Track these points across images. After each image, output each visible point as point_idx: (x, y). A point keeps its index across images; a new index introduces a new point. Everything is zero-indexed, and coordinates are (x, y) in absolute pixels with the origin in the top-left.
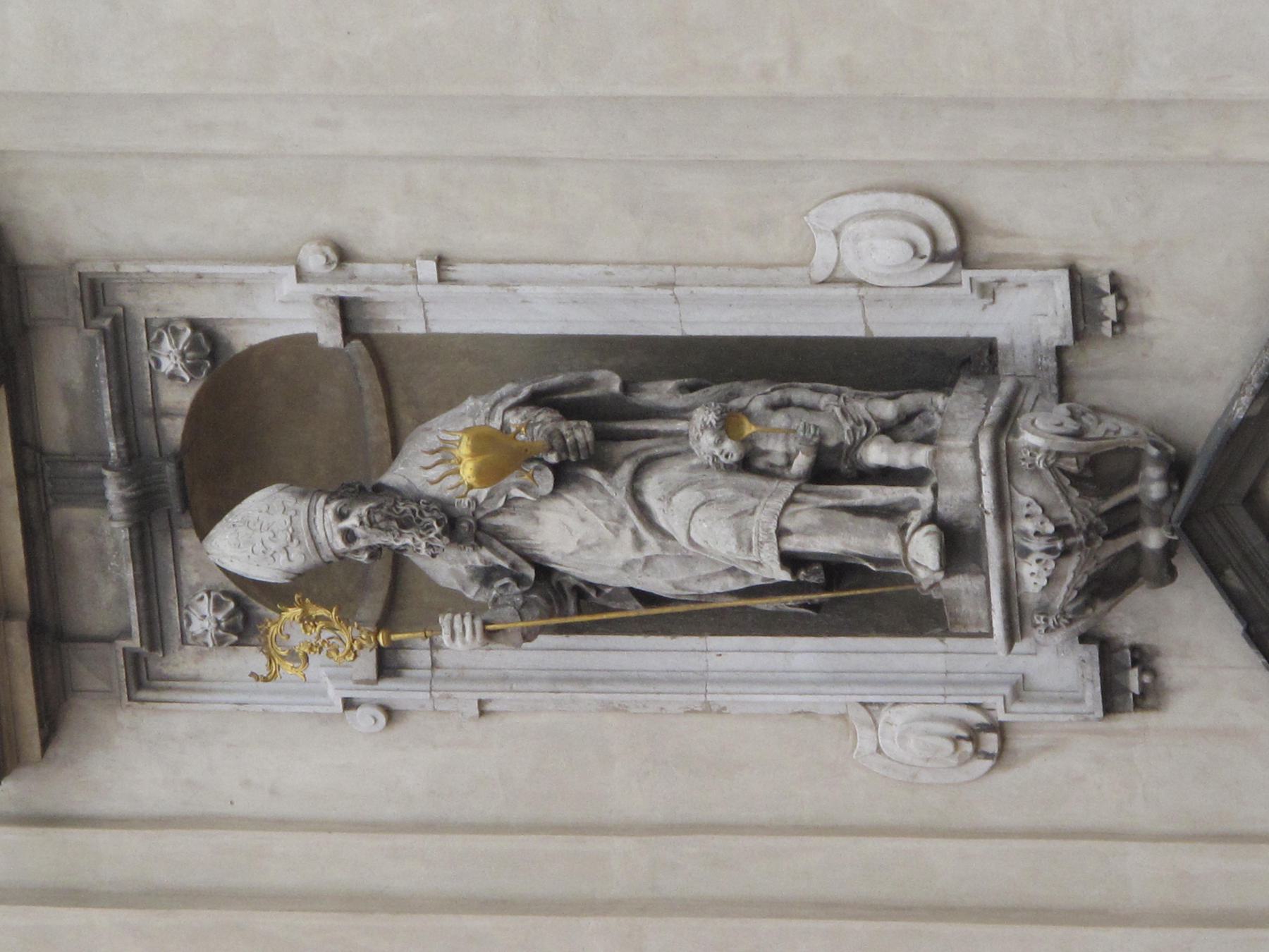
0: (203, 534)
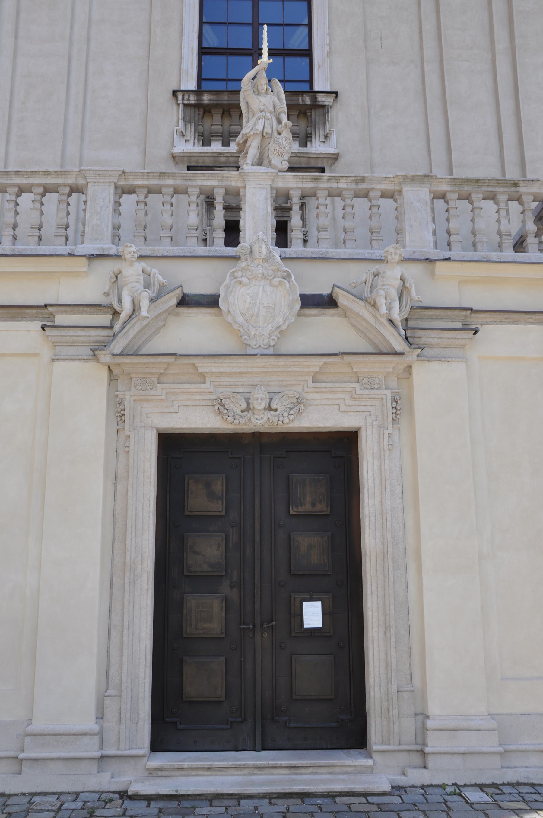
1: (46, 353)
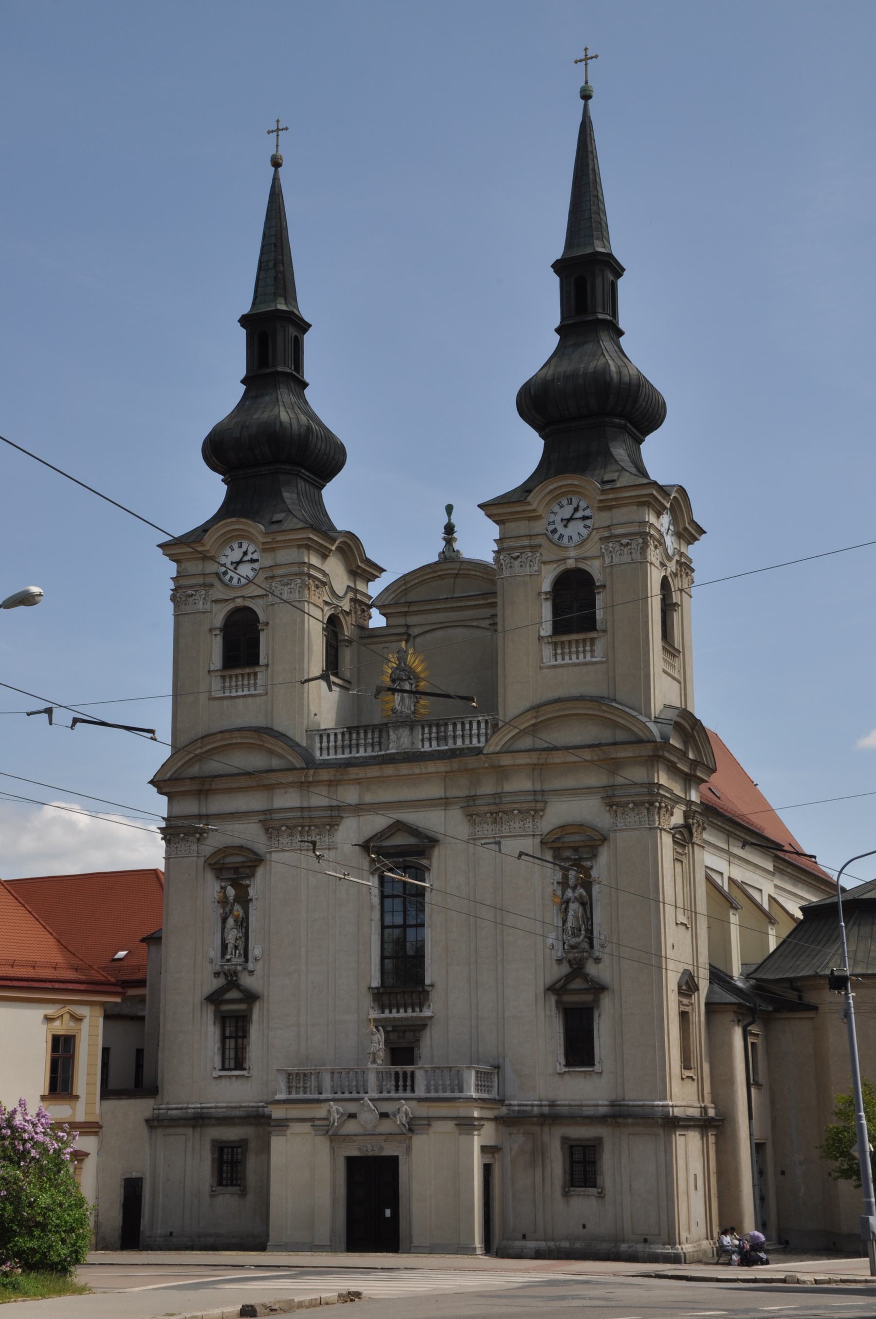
0: (230, 885)
1: (313, 1133)
